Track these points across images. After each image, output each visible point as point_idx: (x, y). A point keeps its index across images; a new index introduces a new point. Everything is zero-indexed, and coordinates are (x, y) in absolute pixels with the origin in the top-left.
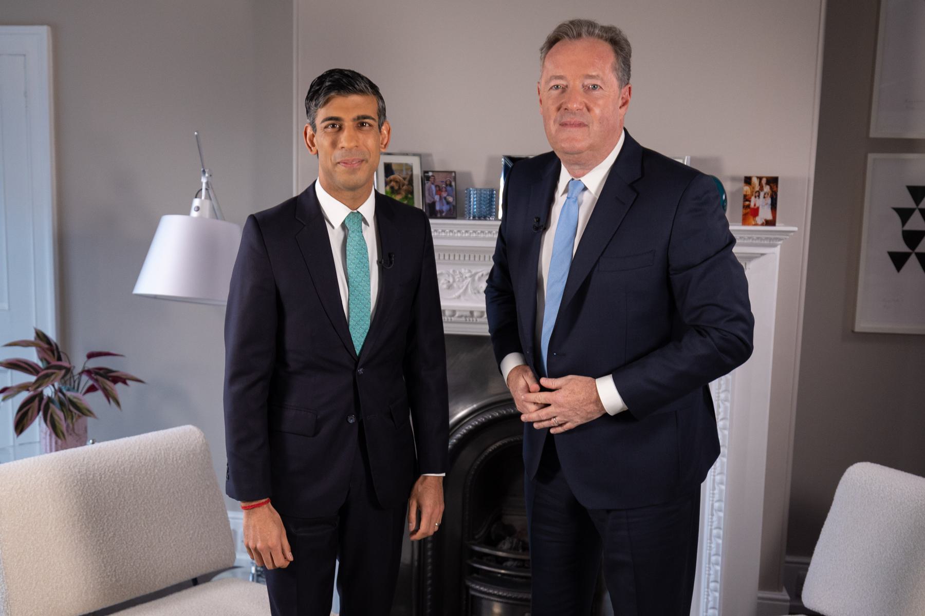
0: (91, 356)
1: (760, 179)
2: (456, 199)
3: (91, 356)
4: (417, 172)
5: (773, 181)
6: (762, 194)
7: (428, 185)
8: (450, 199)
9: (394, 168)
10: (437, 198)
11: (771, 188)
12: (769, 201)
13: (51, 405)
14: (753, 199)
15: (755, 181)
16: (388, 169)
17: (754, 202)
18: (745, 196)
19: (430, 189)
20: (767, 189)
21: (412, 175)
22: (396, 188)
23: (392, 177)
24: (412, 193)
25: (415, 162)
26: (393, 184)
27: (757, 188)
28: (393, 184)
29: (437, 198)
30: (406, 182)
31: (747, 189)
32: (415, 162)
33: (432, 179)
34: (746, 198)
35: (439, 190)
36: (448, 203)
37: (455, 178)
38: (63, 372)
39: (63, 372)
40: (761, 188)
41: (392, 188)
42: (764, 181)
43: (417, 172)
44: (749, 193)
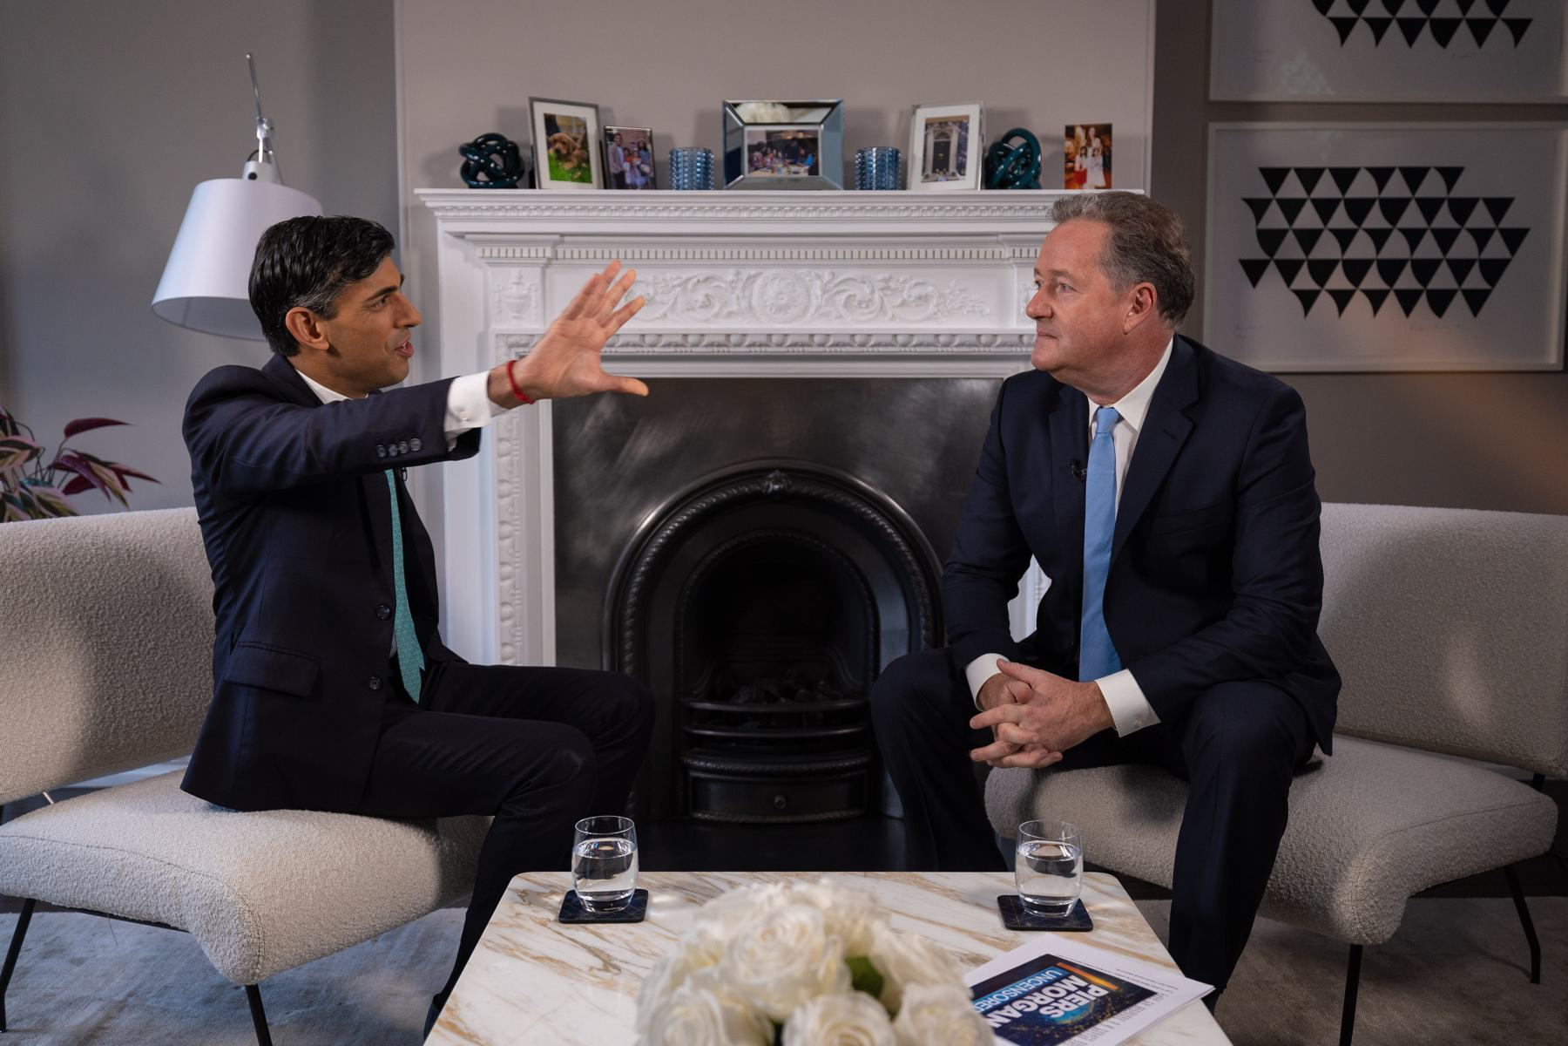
0: (74, 429)
1: (1086, 128)
2: (654, 166)
3: (74, 429)
4: (592, 130)
5: (1104, 131)
6: (1090, 151)
7: (612, 146)
8: (646, 169)
9: (559, 122)
10: (626, 166)
11: (1102, 142)
12: (1100, 160)
13: (9, 505)
14: (1078, 158)
15: (1080, 132)
16: (551, 123)
17: (1079, 162)
18: (1067, 155)
19: (615, 153)
20: (1096, 143)
21: (586, 136)
22: (564, 152)
23: (557, 136)
24: (587, 161)
25: (588, 116)
26: (558, 145)
27: (1083, 143)
28: (558, 145)
29: (626, 166)
30: (578, 145)
31: (1069, 144)
32: (588, 116)
33: (617, 139)
34: (1069, 158)
35: (629, 155)
36: (643, 174)
37: (651, 139)
38: (27, 452)
39: (27, 452)
40: (1089, 143)
41: (557, 151)
42: (1092, 132)
43: (592, 130)
44: (1072, 150)
